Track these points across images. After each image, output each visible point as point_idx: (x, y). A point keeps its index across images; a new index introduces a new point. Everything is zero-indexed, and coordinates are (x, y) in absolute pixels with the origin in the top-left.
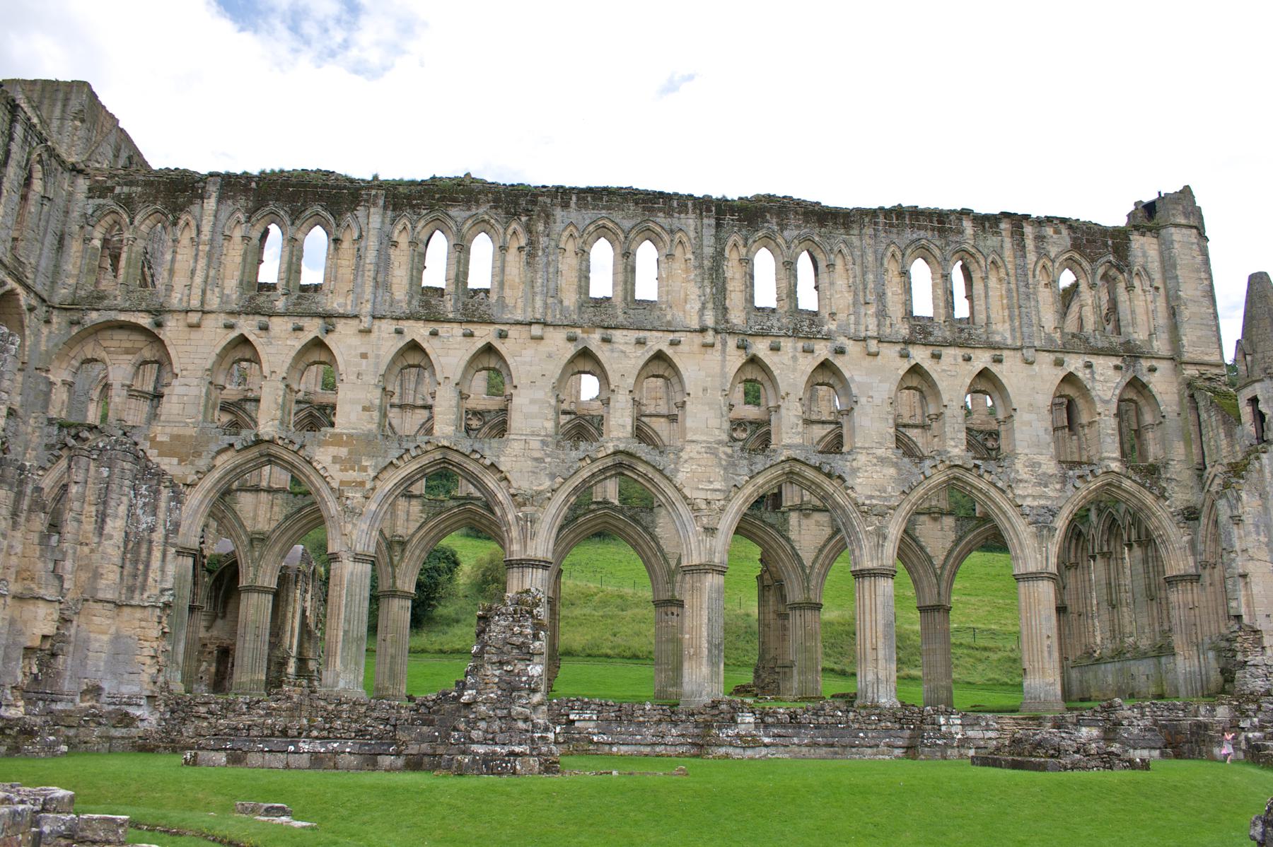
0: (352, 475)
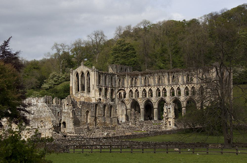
0: (141, 102)
